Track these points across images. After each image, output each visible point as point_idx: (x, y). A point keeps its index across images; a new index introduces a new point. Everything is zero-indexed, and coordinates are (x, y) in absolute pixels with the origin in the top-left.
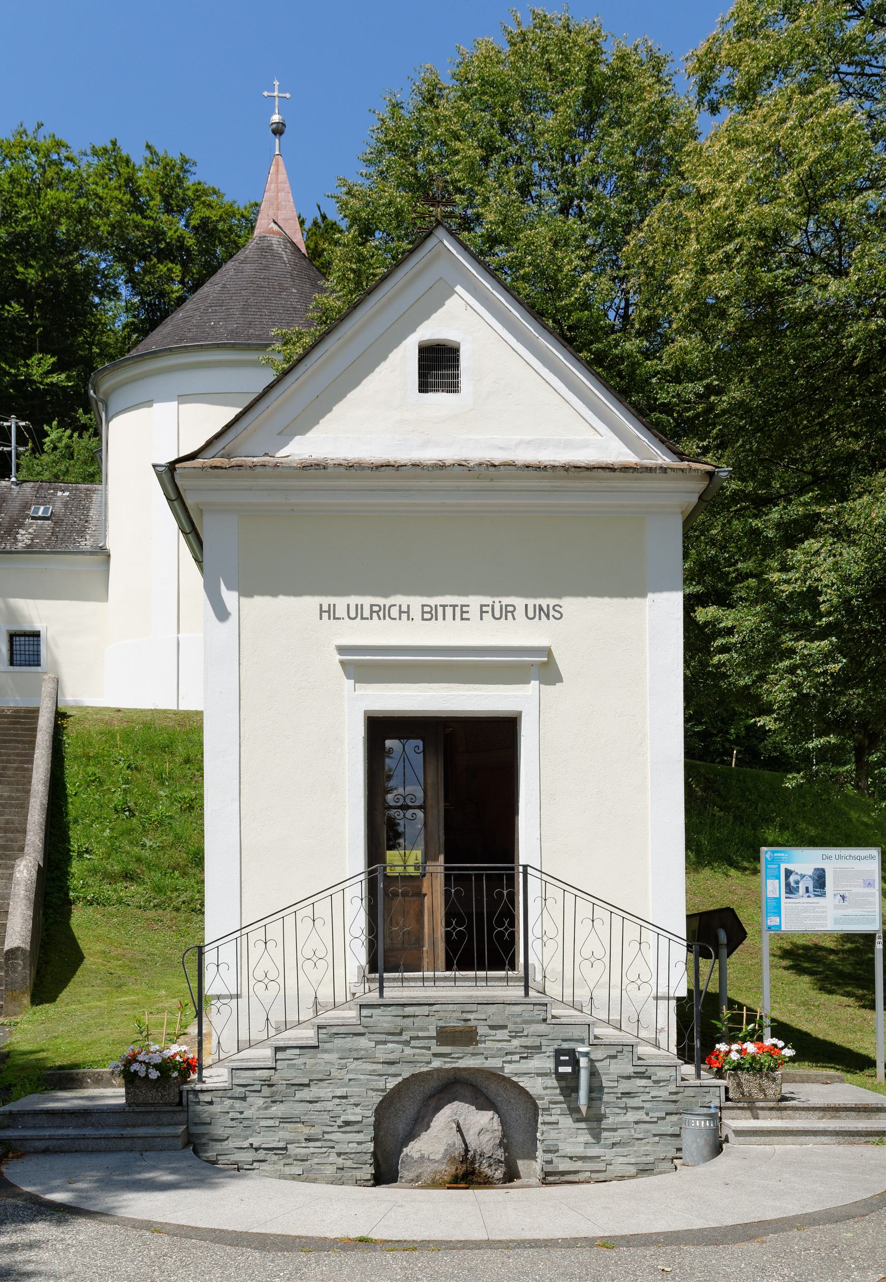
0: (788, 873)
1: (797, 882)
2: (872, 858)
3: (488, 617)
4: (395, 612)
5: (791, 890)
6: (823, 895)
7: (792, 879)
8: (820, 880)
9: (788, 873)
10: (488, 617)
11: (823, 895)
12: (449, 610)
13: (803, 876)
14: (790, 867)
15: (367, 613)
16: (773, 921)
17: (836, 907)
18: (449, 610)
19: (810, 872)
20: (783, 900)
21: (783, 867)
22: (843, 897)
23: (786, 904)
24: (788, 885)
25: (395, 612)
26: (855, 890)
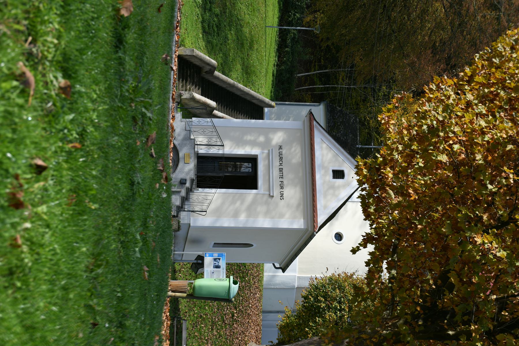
0: (219, 259)
1: (217, 261)
3: (280, 183)
5: (215, 260)
6: (214, 268)
7: (218, 260)
8: (218, 267)
10: (280, 183)
11: (214, 268)
12: (282, 174)
13: (218, 263)
14: (221, 260)
15: (280, 156)
16: (207, 255)
17: (211, 271)
18: (282, 174)
19: (219, 265)
20: (213, 258)
21: (221, 258)
22: (213, 273)
23: (211, 258)
24: (217, 259)
25: (281, 162)
26: (215, 276)
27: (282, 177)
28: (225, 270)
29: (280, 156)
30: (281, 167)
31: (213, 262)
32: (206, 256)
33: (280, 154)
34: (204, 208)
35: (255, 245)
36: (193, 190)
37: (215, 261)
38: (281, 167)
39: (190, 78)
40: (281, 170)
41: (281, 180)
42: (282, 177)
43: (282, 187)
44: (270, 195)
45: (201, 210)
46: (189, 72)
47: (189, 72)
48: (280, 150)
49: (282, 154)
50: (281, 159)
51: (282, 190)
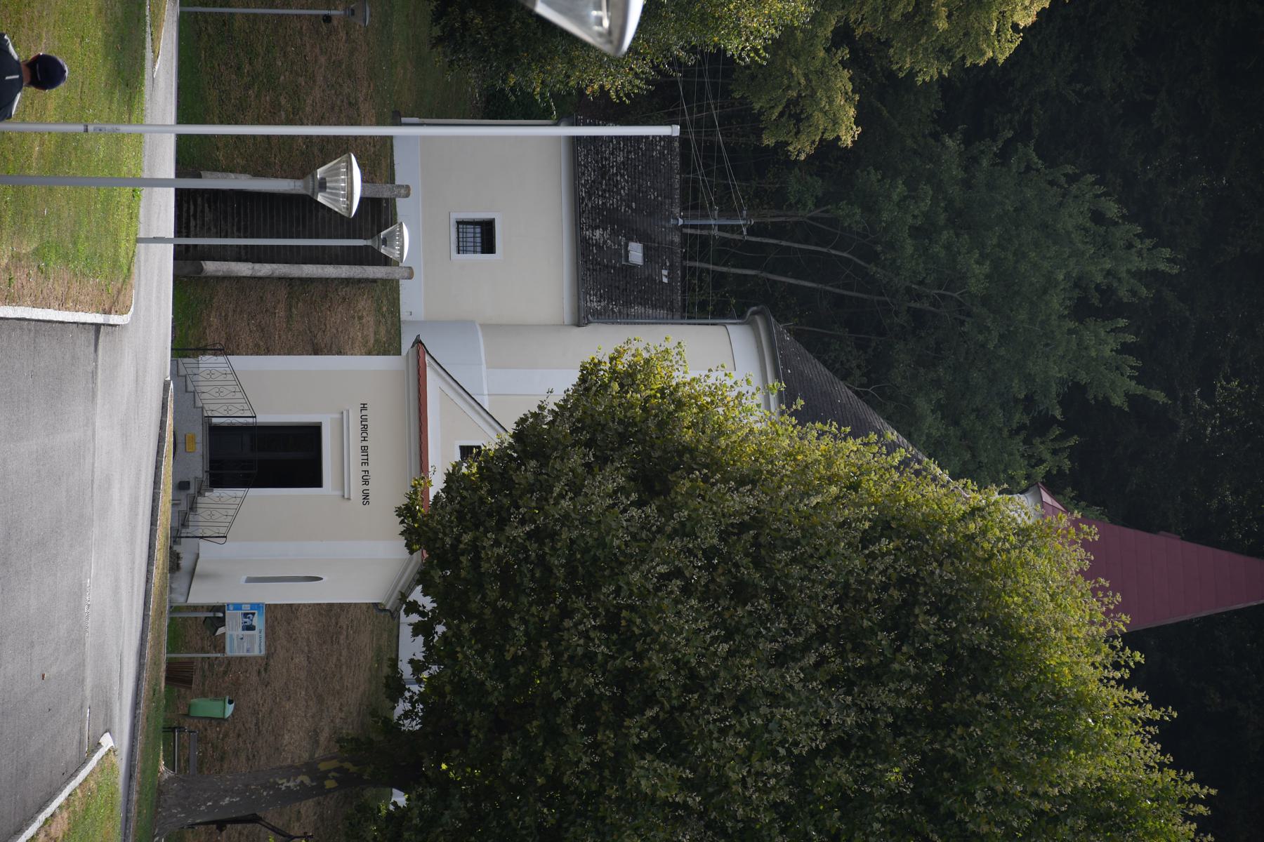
0: (253, 614)
2: (260, 652)
4: (364, 435)
5: (245, 615)
6: (243, 630)
7: (251, 616)
8: (251, 628)
9: (253, 614)
11: (243, 630)
12: (366, 457)
14: (256, 615)
15: (364, 423)
18: (366, 457)
19: (254, 624)
21: (256, 612)
22: (242, 639)
24: (248, 614)
25: (364, 435)
26: (245, 644)
27: (365, 463)
28: (263, 634)
29: (364, 423)
30: (364, 444)
31: (240, 620)
32: (228, 609)
33: (363, 419)
34: (223, 531)
35: (325, 579)
36: (202, 491)
37: (246, 618)
38: (364, 444)
39: (195, 219)
40: (364, 450)
41: (365, 468)
42: (365, 463)
43: (366, 482)
44: (343, 496)
45: (217, 535)
46: (192, 207)
47: (192, 207)
48: (364, 412)
49: (366, 420)
50: (365, 428)
51: (365, 487)
